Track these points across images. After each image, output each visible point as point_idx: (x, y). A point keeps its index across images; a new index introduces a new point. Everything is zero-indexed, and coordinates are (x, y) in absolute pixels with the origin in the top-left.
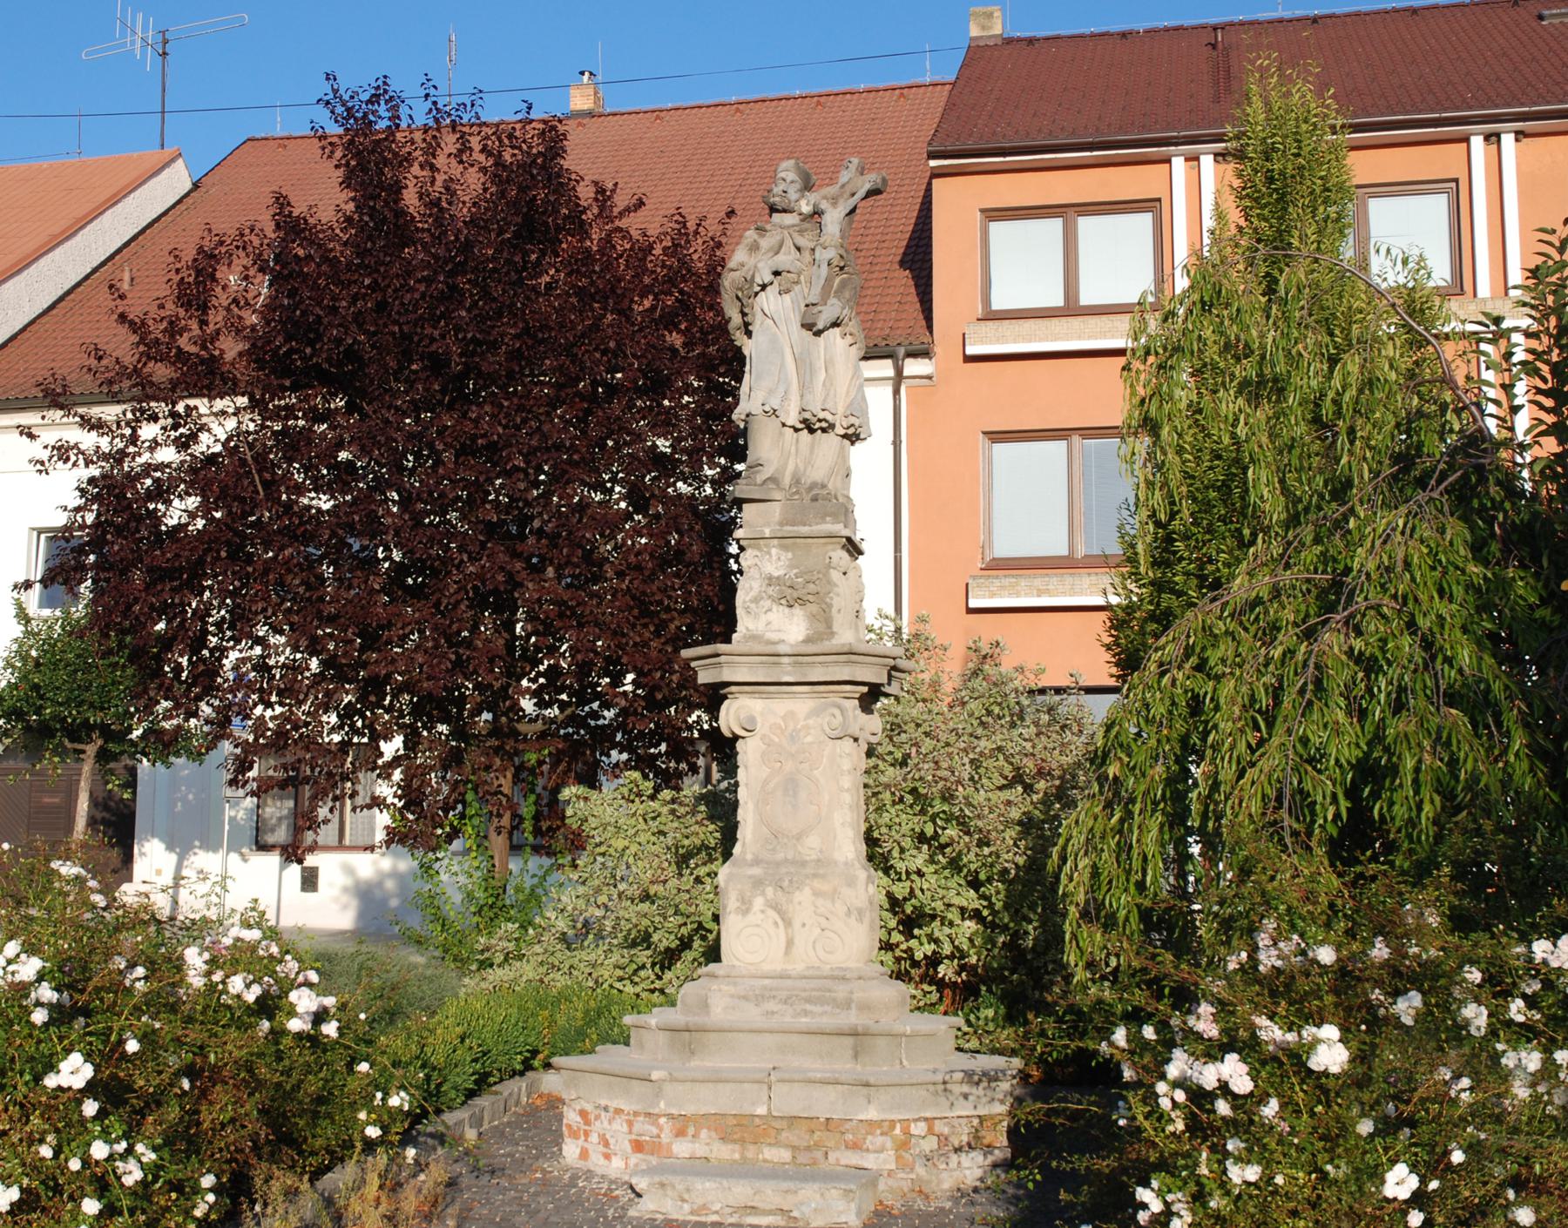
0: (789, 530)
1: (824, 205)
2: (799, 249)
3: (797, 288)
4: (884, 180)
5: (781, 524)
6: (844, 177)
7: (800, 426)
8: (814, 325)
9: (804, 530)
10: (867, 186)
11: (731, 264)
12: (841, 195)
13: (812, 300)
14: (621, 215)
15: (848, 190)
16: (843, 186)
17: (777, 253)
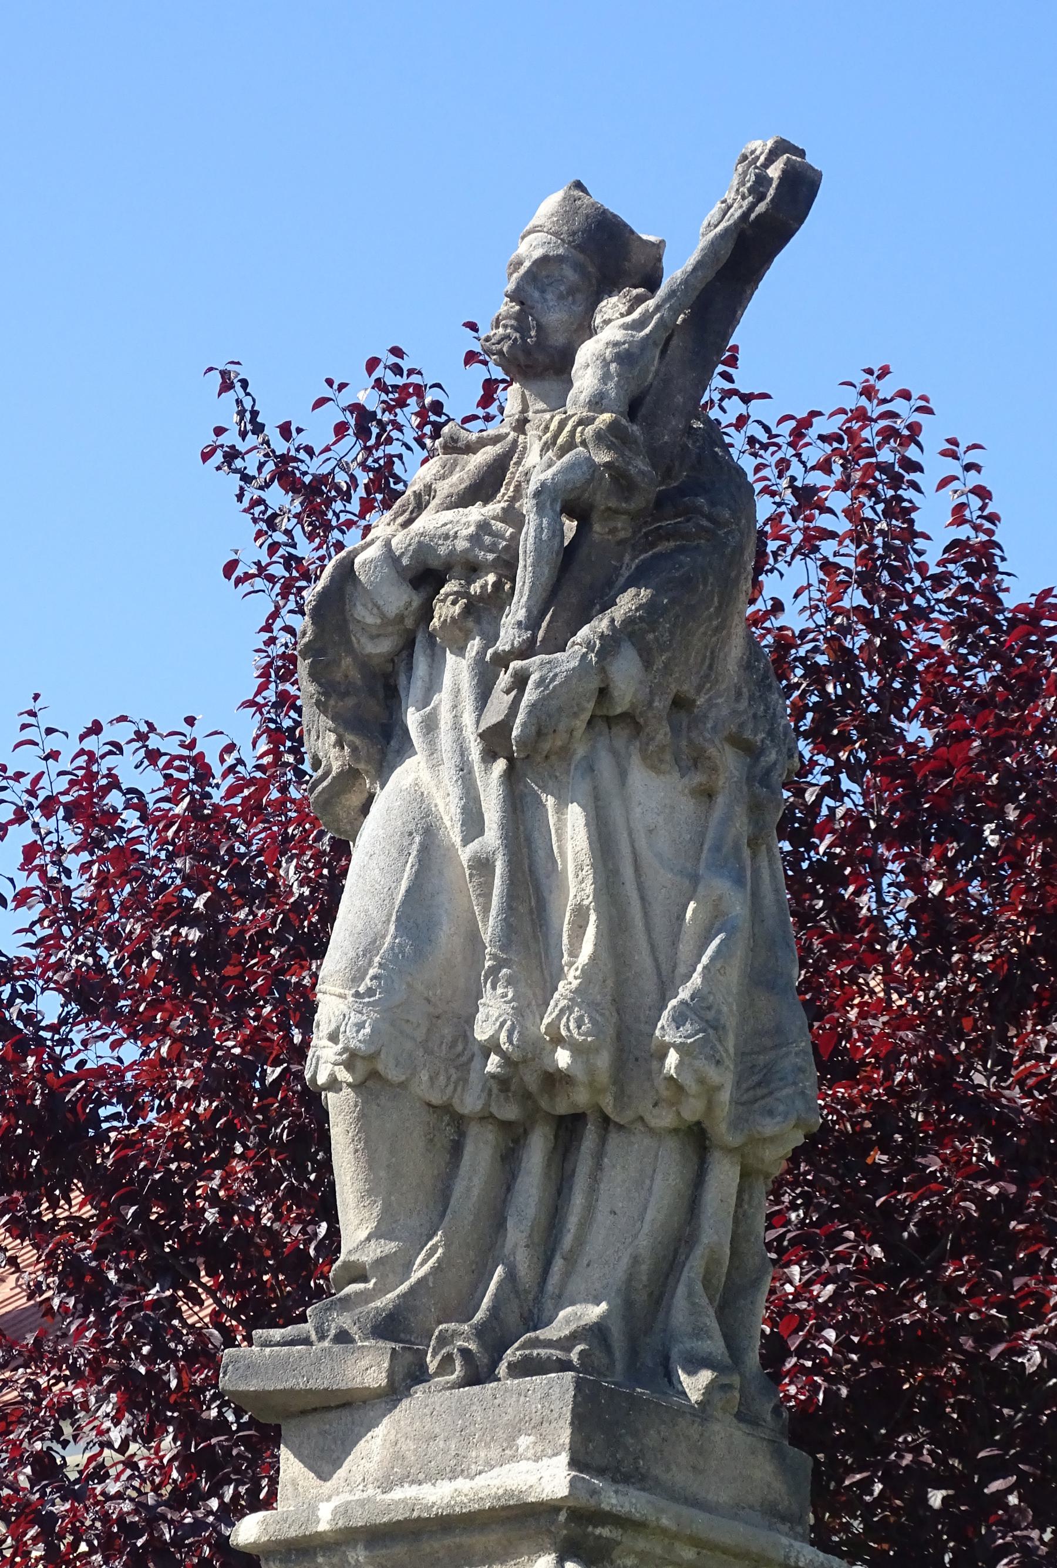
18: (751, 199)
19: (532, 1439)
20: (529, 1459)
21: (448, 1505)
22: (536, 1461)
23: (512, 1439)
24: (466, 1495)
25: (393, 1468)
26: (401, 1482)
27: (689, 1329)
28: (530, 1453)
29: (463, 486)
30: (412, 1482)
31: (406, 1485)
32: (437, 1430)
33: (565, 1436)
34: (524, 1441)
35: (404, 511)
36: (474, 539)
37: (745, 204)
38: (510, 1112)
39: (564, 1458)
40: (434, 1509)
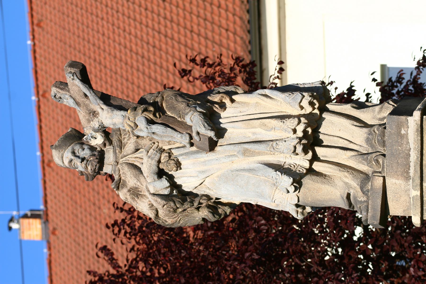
0: (413, 171)
1: (95, 124)
2: (137, 150)
3: (175, 153)
4: (73, 65)
5: (407, 178)
6: (70, 103)
7: (310, 154)
8: (210, 139)
9: (414, 156)
10: (78, 82)
11: (151, 214)
12: (86, 106)
13: (185, 140)
14: (116, 266)
15: (81, 99)
16: (77, 104)
17: (141, 172)
18: (75, 76)
19: (402, 129)
20: (408, 130)
21: (418, 151)
22: (408, 127)
23: (402, 137)
24: (416, 145)
25: (404, 176)
26: (408, 173)
27: (372, 113)
28: (406, 129)
29: (134, 171)
30: (409, 169)
31: (410, 171)
32: (396, 161)
33: (403, 118)
34: (403, 132)
35: (134, 198)
36: (152, 159)
37: (75, 77)
38: (310, 155)
39: (409, 118)
40: (418, 156)
